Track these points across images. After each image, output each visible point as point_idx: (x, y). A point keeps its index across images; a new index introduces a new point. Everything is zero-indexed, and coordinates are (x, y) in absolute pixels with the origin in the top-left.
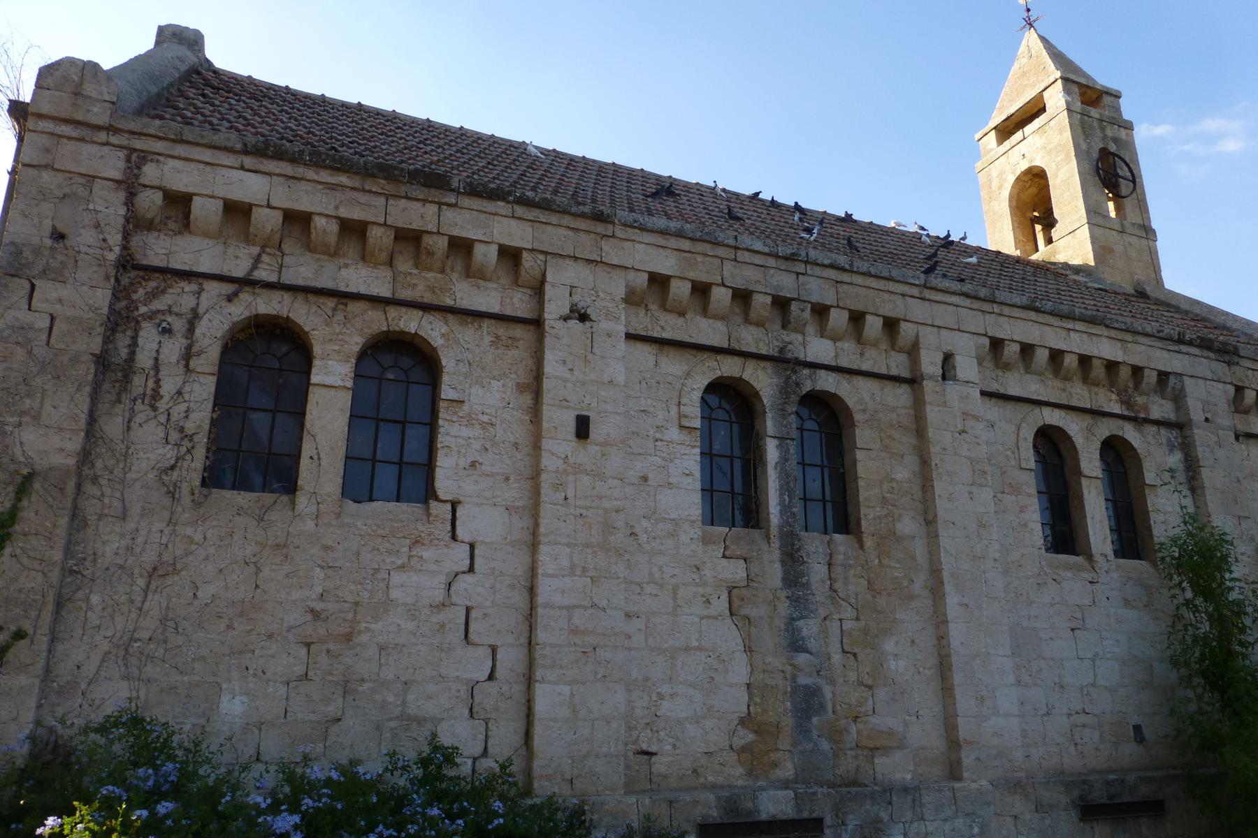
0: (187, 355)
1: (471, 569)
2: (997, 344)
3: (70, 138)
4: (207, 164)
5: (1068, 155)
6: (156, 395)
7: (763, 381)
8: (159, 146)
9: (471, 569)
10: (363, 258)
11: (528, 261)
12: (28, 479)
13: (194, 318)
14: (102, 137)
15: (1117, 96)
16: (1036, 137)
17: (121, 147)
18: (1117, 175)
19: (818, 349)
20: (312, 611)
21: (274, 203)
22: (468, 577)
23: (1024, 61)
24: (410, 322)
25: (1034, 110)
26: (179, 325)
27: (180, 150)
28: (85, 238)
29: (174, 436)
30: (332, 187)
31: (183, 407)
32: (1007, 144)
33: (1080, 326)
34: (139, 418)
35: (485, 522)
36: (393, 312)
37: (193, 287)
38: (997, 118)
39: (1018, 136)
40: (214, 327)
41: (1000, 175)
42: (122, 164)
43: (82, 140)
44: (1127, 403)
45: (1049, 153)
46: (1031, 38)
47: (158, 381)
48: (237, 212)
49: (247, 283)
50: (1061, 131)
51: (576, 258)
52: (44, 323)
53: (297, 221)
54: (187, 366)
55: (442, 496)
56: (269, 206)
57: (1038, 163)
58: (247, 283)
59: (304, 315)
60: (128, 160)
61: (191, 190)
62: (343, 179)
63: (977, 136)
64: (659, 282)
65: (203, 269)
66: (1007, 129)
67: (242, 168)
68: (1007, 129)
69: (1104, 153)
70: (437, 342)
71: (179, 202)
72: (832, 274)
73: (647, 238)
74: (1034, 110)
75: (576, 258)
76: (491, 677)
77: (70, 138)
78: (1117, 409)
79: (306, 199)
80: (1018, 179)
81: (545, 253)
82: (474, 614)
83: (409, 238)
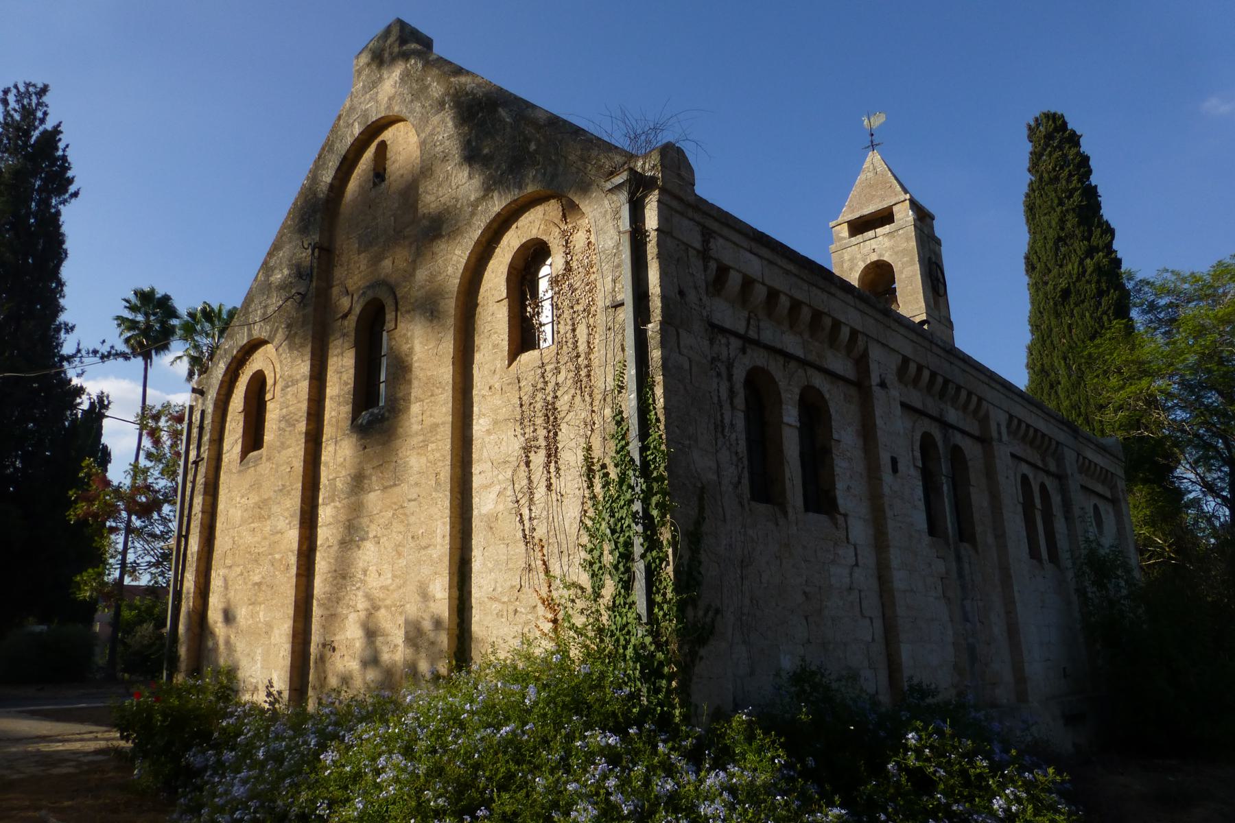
0: (732, 393)
1: (857, 565)
2: (1011, 417)
3: (677, 211)
4: (735, 243)
5: (912, 259)
6: (723, 428)
7: (937, 435)
8: (715, 226)
9: (857, 565)
10: (791, 327)
11: (861, 341)
12: (703, 488)
13: (730, 366)
14: (690, 213)
15: (933, 218)
16: (886, 239)
17: (699, 223)
18: (938, 280)
19: (953, 416)
20: (805, 593)
21: (767, 281)
22: (856, 569)
23: (870, 175)
24: (818, 381)
25: (884, 217)
26: (723, 370)
27: (726, 231)
28: (692, 296)
29: (735, 458)
30: (787, 272)
31: (734, 436)
32: (859, 238)
33: (1035, 410)
34: (719, 443)
35: (859, 531)
36: (810, 371)
37: (723, 341)
38: (849, 214)
39: (871, 234)
40: (739, 374)
41: (852, 260)
42: (699, 238)
43: (682, 214)
44: (1043, 460)
45: (896, 253)
46: (874, 160)
47: (722, 415)
48: (748, 283)
49: (744, 338)
50: (908, 240)
51: (878, 342)
52: (687, 366)
53: (773, 295)
54: (732, 403)
55: (842, 510)
56: (763, 284)
57: (886, 258)
58: (748, 342)
59: (775, 368)
60: (703, 235)
61: (731, 264)
62: (791, 267)
63: (831, 224)
64: (906, 361)
65: (727, 325)
66: (860, 226)
67: (751, 252)
68: (860, 226)
69: (930, 259)
70: (827, 396)
71: (723, 270)
72: (961, 364)
73: (902, 330)
74: (884, 217)
75: (878, 342)
76: (873, 639)
77: (677, 211)
78: (1040, 464)
79: (779, 282)
80: (867, 267)
81: (868, 336)
82: (863, 594)
83: (817, 315)
